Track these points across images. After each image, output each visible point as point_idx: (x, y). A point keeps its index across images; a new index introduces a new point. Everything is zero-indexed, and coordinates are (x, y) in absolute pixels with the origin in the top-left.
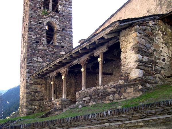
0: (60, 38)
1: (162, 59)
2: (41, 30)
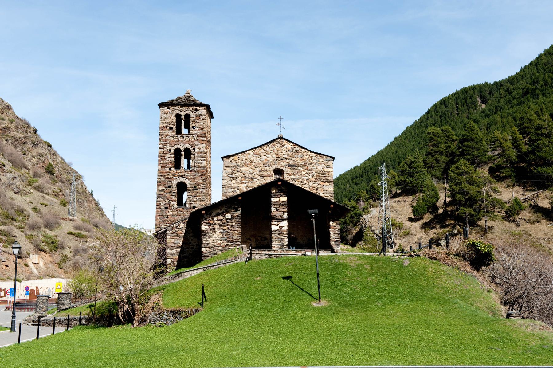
0: (190, 198)
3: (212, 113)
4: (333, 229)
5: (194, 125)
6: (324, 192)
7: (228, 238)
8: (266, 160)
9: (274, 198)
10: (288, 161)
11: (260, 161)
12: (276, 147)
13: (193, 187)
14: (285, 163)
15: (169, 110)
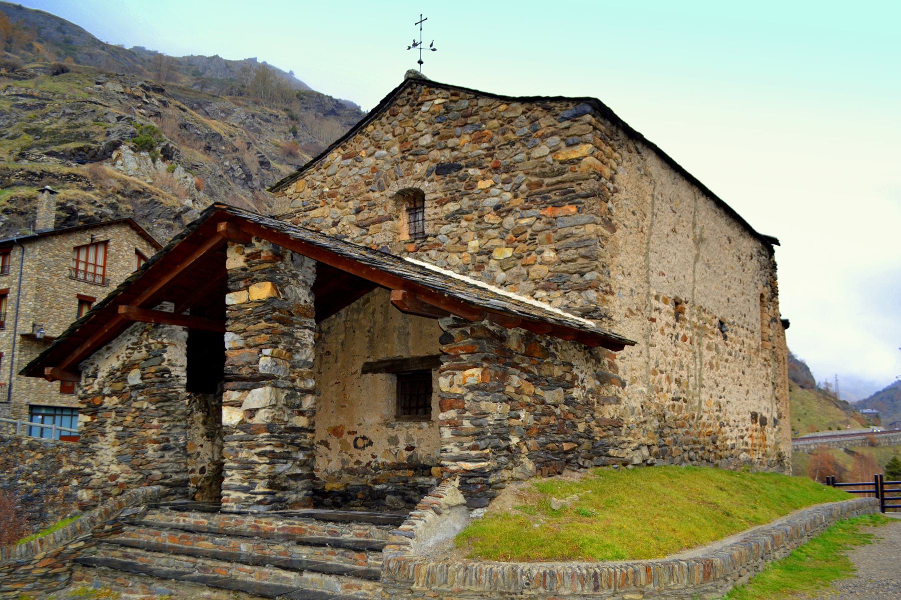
4: (451, 414)
6: (557, 245)
8: (374, 169)
10: (435, 154)
11: (357, 177)
12: (400, 116)
14: (426, 165)
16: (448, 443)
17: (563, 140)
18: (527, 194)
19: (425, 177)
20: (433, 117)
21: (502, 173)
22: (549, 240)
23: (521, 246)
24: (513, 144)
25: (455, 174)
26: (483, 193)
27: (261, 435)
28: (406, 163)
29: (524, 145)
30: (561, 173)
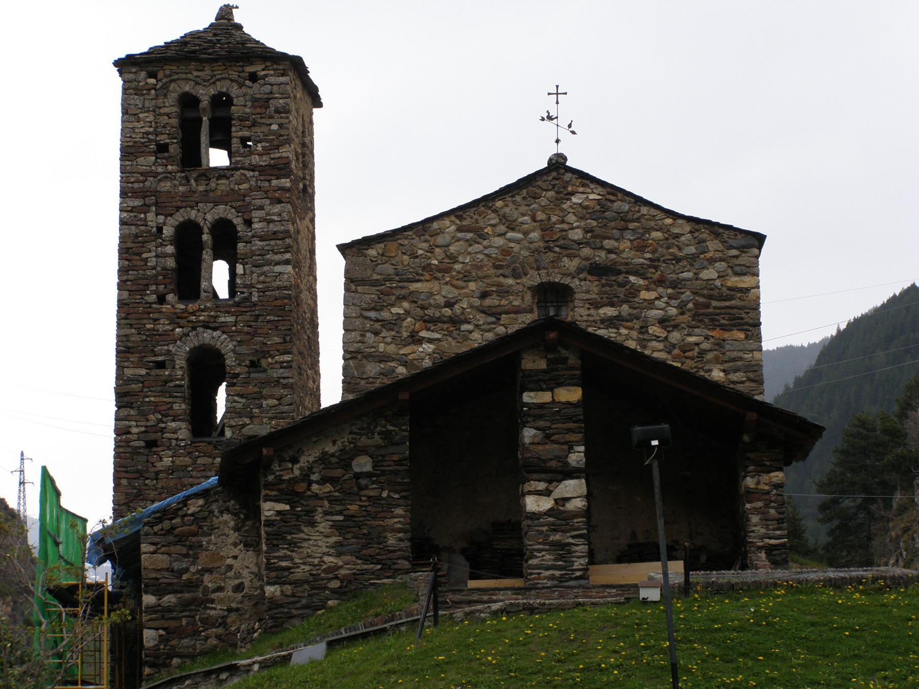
0: (239, 406)
1: (230, 589)
2: (163, 393)
3: (316, 89)
4: (759, 504)
5: (246, 133)
6: (726, 365)
7: (366, 546)
8: (506, 252)
9: (532, 394)
10: (586, 251)
12: (543, 201)
13: (248, 362)
14: (576, 262)
15: (152, 81)
16: (755, 526)
17: (731, 267)
18: (693, 312)
19: (575, 275)
20: (585, 211)
21: (668, 288)
22: (717, 360)
23: (688, 361)
24: (678, 260)
25: (613, 278)
26: (645, 304)
27: (575, 521)
28: (551, 254)
29: (692, 265)
30: (731, 298)
